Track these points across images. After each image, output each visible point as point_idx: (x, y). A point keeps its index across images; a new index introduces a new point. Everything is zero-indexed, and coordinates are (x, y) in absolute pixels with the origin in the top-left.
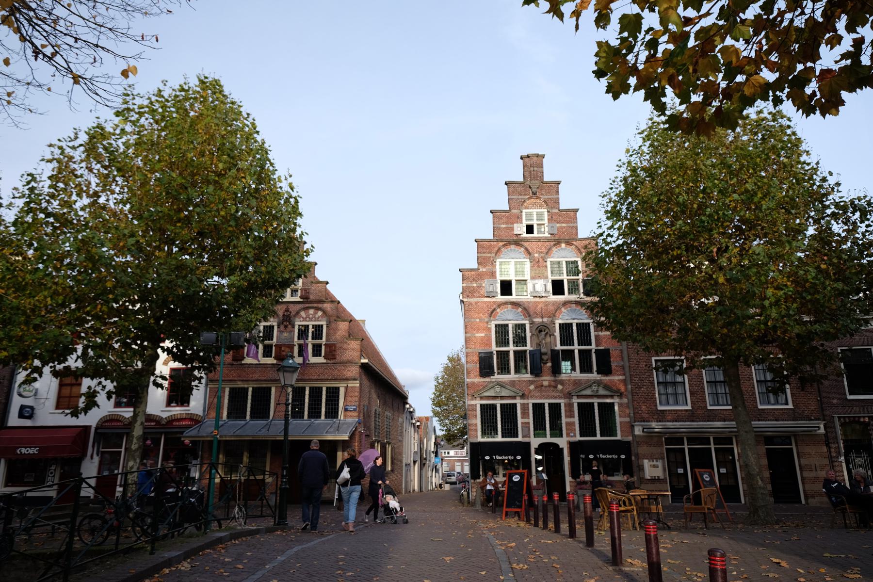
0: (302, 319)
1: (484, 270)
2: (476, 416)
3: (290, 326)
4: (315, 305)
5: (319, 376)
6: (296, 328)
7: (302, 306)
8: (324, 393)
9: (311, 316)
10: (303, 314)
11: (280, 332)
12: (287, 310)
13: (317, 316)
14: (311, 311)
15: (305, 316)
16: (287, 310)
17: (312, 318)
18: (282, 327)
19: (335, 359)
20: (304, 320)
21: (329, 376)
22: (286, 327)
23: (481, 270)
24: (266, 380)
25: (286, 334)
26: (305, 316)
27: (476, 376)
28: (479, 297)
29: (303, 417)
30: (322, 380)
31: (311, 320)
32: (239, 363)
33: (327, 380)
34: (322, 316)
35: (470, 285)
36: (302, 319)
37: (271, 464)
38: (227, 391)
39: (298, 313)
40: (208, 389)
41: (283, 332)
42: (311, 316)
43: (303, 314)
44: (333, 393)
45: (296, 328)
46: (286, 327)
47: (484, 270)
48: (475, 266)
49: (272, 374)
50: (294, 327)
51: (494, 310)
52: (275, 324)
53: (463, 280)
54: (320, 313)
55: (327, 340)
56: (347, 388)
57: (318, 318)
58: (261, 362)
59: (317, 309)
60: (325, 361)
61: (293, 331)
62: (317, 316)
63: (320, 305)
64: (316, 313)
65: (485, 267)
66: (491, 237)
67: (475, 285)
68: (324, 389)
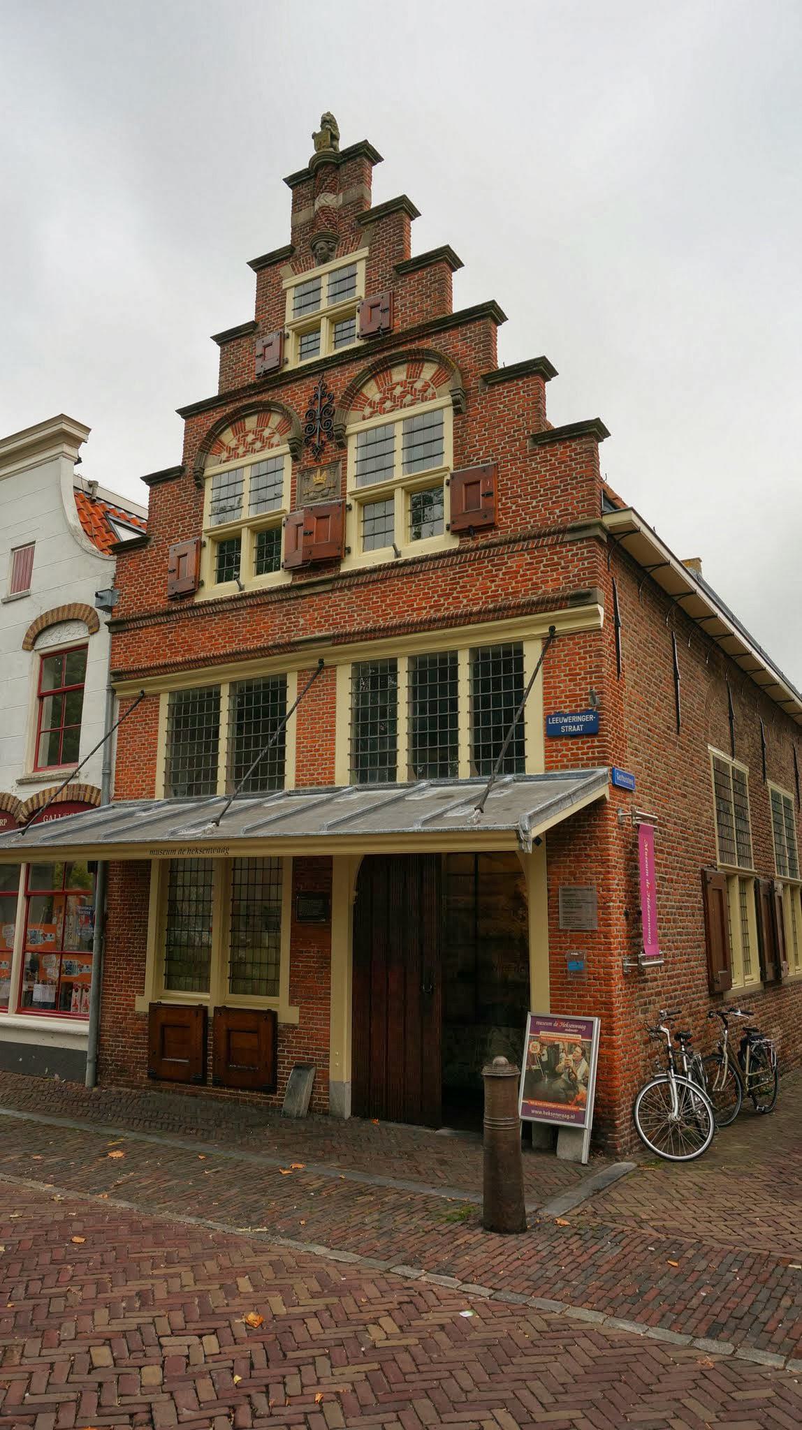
0: (368, 410)
3: (331, 446)
5: (437, 607)
7: (370, 361)
11: (302, 473)
14: (399, 374)
17: (403, 395)
18: (307, 457)
19: (492, 527)
20: (378, 409)
21: (474, 601)
22: (319, 451)
24: (264, 651)
25: (318, 477)
29: (393, 775)
30: (450, 621)
31: (399, 404)
33: (468, 618)
34: (436, 380)
36: (368, 410)
37: (294, 955)
38: (165, 700)
39: (353, 394)
40: (118, 704)
41: (311, 471)
43: (372, 391)
49: (275, 627)
50: (343, 446)
54: (429, 371)
55: (457, 464)
56: (550, 640)
57: (427, 385)
58: (247, 591)
59: (417, 359)
63: (429, 344)
64: (415, 376)
68: (464, 660)
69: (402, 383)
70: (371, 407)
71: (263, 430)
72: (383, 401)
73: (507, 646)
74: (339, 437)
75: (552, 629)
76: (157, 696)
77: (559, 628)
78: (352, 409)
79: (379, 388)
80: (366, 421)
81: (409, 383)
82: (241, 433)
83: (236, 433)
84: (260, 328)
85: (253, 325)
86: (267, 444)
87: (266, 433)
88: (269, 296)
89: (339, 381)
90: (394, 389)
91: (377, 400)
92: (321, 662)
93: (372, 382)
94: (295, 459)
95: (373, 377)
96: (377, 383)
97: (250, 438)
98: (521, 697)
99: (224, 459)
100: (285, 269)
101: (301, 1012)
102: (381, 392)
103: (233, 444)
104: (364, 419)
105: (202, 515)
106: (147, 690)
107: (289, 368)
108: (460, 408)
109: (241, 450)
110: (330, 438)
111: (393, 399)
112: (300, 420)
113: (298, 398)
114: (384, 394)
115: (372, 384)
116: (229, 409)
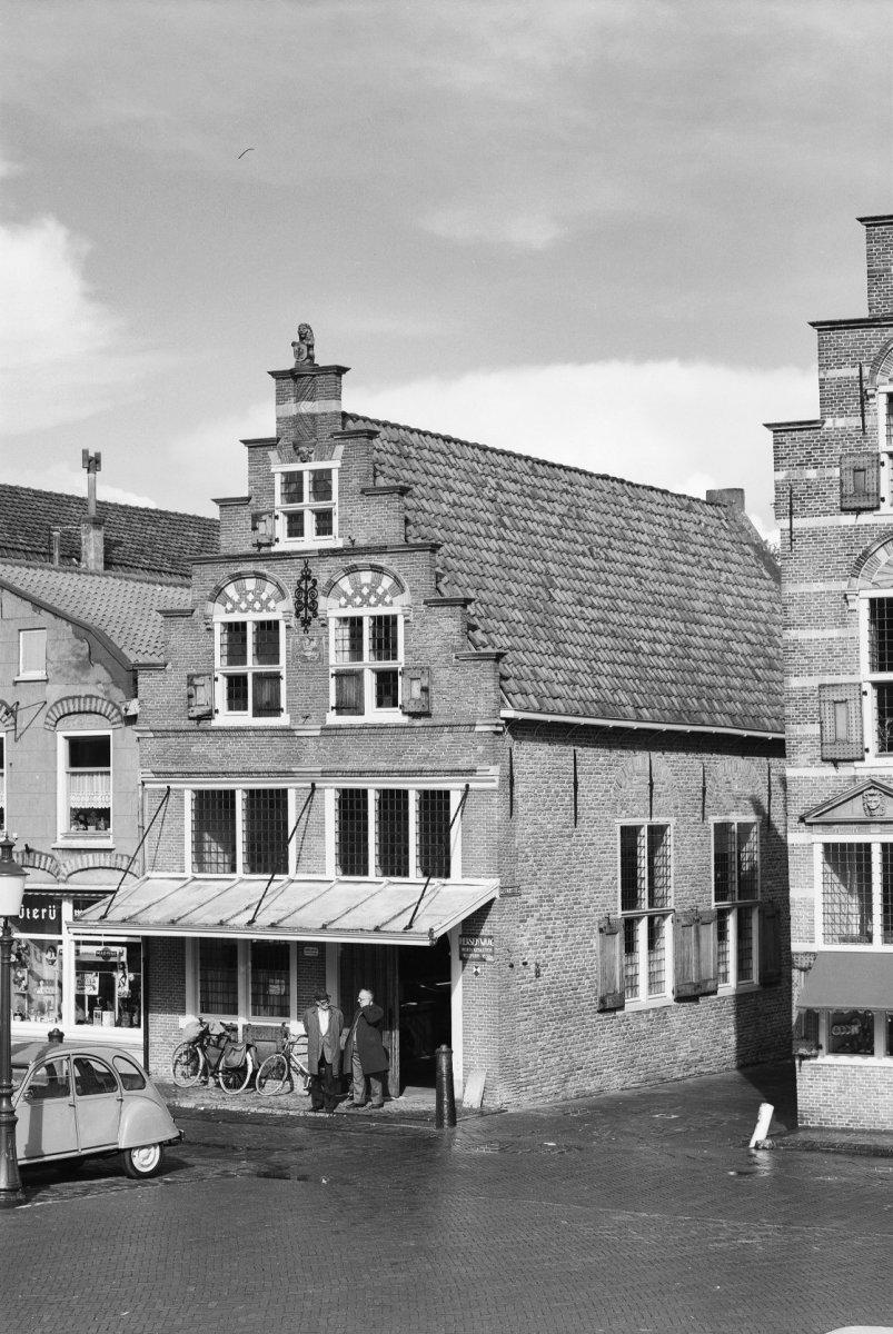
1: (840, 422)
2: (812, 878)
8: (413, 807)
10: (345, 584)
13: (380, 591)
16: (306, 577)
23: (829, 422)
27: (812, 760)
28: (825, 513)
31: (365, 601)
32: (203, 724)
35: (795, 474)
36: (343, 601)
38: (188, 797)
44: (435, 803)
47: (840, 422)
48: (813, 413)
51: (866, 555)
53: (777, 459)
57: (385, 593)
60: (405, 720)
62: (380, 591)
65: (842, 413)
66: (864, 314)
67: (812, 474)
72: (354, 596)
73: (440, 792)
75: (467, 786)
76: (181, 791)
77: (472, 786)
84: (252, 502)
85: (249, 499)
86: (265, 606)
92: (313, 785)
93: (346, 577)
97: (250, 597)
98: (449, 828)
100: (273, 455)
103: (236, 598)
106: (172, 786)
107: (276, 548)
109: (243, 606)
111: (362, 596)
112: (290, 593)
113: (290, 575)
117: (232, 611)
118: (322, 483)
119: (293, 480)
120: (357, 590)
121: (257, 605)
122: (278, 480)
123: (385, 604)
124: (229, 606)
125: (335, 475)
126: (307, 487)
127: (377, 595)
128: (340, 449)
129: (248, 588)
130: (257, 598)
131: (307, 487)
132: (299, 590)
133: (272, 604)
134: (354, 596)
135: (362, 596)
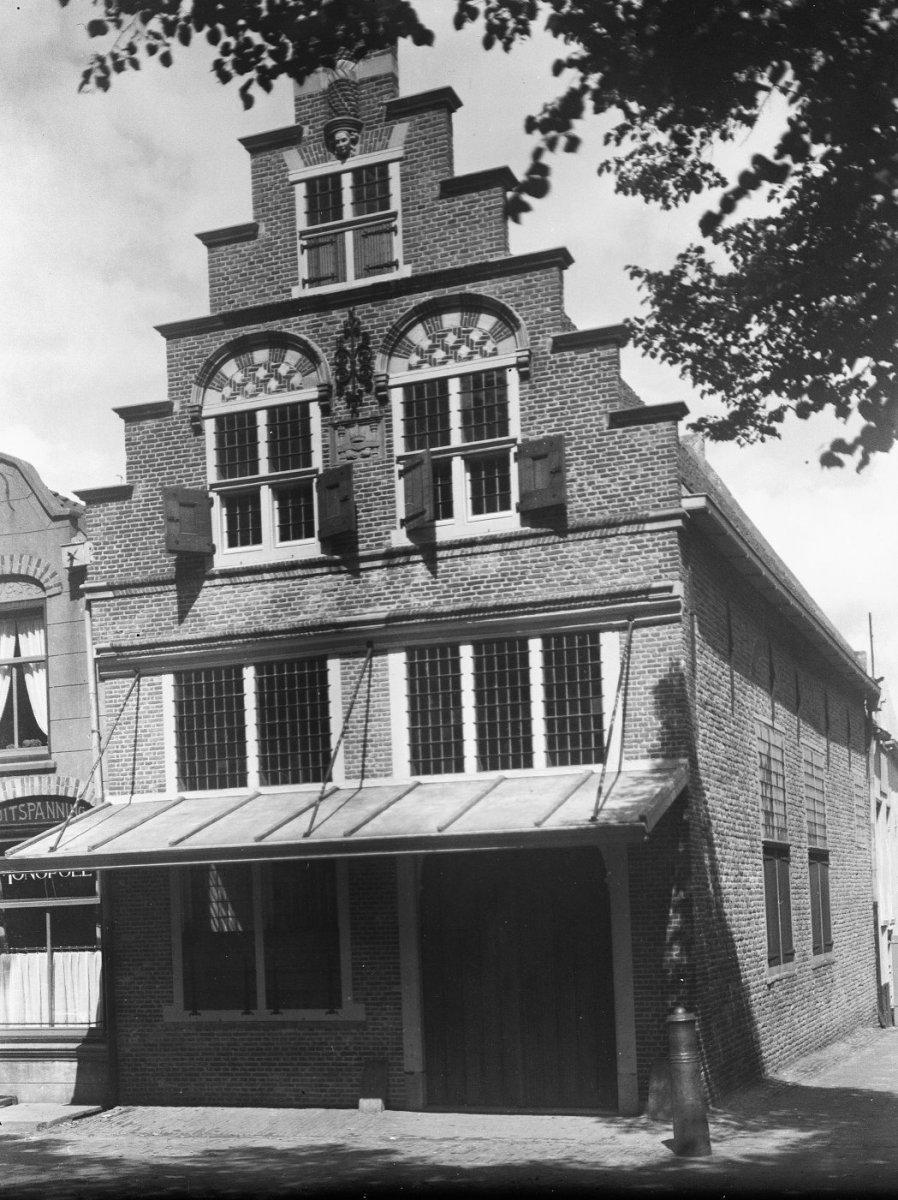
3: (369, 398)
4: (469, 288)
6: (397, 397)
9: (451, 339)
12: (352, 330)
13: (475, 336)
14: (451, 320)
15: (426, 344)
18: (340, 406)
20: (426, 357)
22: (354, 401)
26: (426, 344)
31: (452, 353)
36: (415, 359)
42: (451, 339)
43: (418, 335)
45: (397, 397)
46: (354, 401)
50: (384, 401)
52: (312, 393)
59: (473, 306)
61: (381, 419)
62: (475, 336)
63: (485, 289)
69: (455, 330)
70: (418, 354)
71: (278, 366)
72: (432, 349)
74: (380, 389)
78: (395, 356)
79: (428, 334)
80: (412, 372)
81: (464, 332)
82: (249, 369)
83: (241, 367)
87: (283, 370)
88: (269, 193)
89: (377, 319)
90: (445, 336)
91: (426, 348)
94: (326, 411)
95: (420, 320)
96: (424, 326)
97: (261, 373)
99: (227, 396)
101: (367, 1009)
102: (429, 338)
103: (239, 377)
104: (411, 368)
105: (205, 463)
108: (527, 373)
109: (250, 387)
110: (368, 391)
112: (326, 359)
114: (434, 341)
115: (419, 327)
116: (230, 335)
117: (234, 396)
118: (371, 183)
119: (323, 194)
120: (437, 340)
121: (273, 384)
122: (301, 191)
123: (484, 354)
124: (227, 391)
125: (394, 170)
126: (347, 196)
127: (470, 343)
128: (401, 129)
129: (257, 362)
130: (273, 372)
131: (347, 196)
132: (341, 353)
133: (296, 379)
134: (432, 349)
135: (445, 348)
